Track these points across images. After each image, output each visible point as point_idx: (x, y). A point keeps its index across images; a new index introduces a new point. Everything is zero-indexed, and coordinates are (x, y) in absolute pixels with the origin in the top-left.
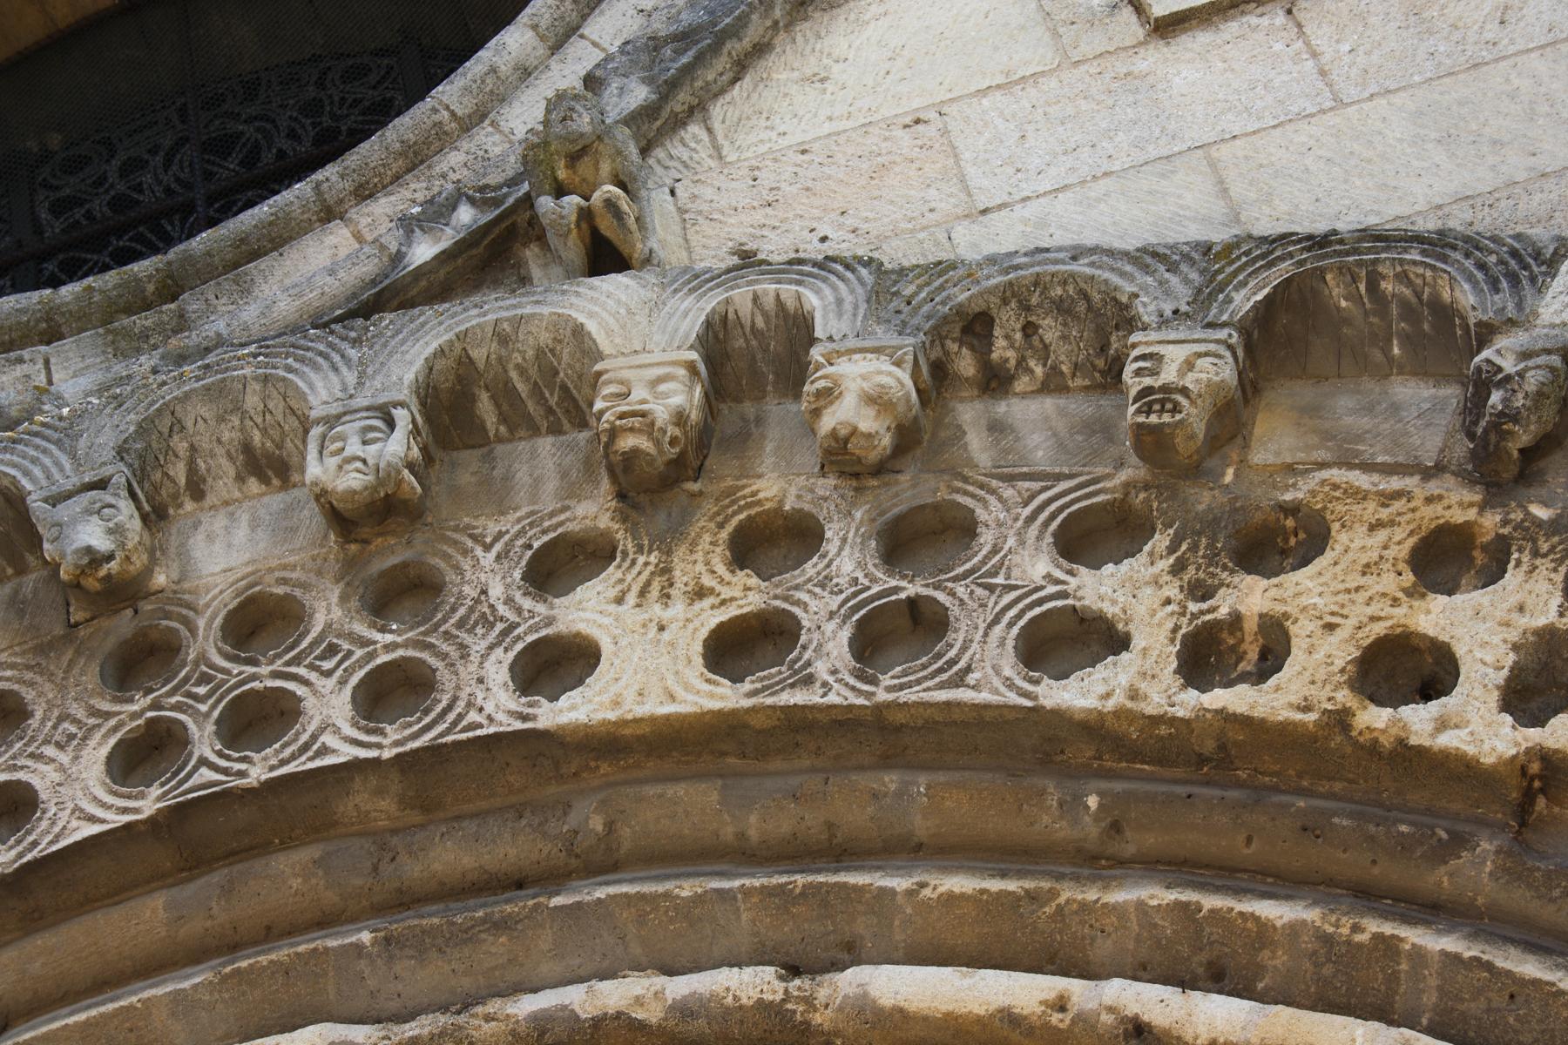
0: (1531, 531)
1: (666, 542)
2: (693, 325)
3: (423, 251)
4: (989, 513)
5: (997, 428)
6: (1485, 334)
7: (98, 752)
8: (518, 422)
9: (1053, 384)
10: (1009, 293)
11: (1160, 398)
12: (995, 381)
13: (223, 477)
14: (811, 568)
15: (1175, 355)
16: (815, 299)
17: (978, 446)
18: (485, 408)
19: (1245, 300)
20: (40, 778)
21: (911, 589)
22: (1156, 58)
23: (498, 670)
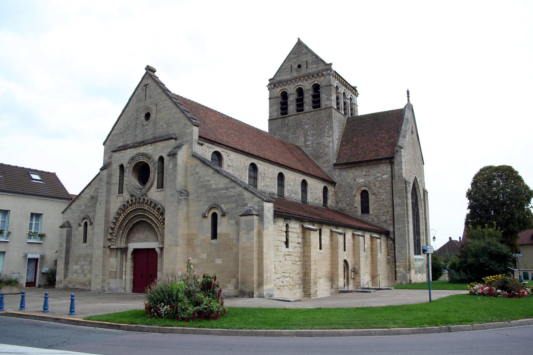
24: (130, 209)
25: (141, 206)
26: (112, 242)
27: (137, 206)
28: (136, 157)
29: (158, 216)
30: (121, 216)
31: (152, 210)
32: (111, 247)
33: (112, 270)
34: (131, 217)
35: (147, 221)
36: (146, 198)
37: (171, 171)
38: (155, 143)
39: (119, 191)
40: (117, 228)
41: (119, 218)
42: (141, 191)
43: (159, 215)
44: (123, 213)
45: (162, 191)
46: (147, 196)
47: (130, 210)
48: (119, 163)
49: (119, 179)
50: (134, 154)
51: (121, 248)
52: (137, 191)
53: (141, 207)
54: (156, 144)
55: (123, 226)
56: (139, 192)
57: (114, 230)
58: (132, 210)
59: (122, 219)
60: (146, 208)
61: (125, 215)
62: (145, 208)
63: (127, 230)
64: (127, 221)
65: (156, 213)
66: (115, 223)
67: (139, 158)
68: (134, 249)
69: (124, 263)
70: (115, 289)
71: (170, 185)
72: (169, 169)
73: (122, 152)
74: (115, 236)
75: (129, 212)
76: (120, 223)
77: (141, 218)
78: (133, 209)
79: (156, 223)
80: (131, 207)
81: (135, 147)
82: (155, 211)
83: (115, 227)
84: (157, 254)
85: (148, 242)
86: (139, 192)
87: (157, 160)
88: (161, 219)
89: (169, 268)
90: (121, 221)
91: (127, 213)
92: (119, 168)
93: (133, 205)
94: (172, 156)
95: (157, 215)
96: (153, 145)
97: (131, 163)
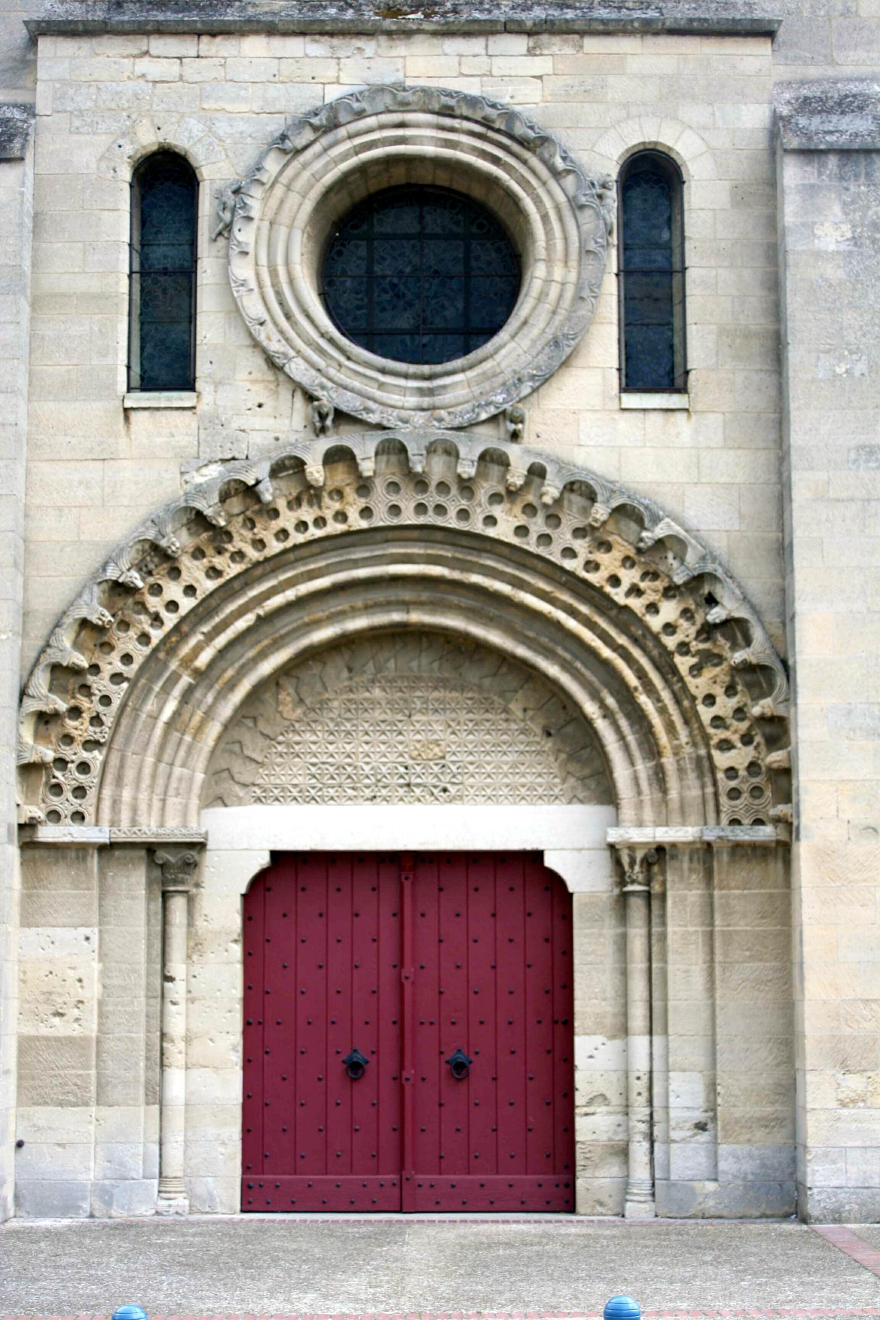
0: (640, 562)
1: (513, 502)
2: (527, 466)
3: (484, 416)
4: (564, 521)
5: (570, 501)
6: (644, 529)
7: (413, 505)
8: (492, 461)
9: (581, 495)
10: (580, 482)
11: (596, 520)
12: (572, 491)
13: (440, 451)
14: (534, 520)
15: (601, 511)
16: (549, 469)
17: (566, 503)
18: (488, 458)
19: (615, 504)
20: (402, 506)
21: (548, 531)
22: (619, 416)
23: (481, 518)
24: (302, 526)
25: (440, 509)
26: (57, 789)
27: (395, 510)
28: (360, 115)
29: (637, 604)
30: (175, 573)
31: (569, 553)
32: (48, 833)
33: (60, 1028)
34: (290, 594)
35: (478, 631)
36: (513, 451)
37: (834, 272)
38: (582, 33)
39: (129, 367)
40: (117, 678)
41: (157, 590)
42: (421, 392)
43: (650, 597)
44: (198, 553)
45: (681, 417)
46: (515, 436)
47: (297, 538)
48: (129, 133)
49: (127, 271)
50: (333, 94)
51: (150, 849)
52: (381, 386)
53: (430, 519)
54: (591, 44)
55: (186, 662)
56: (412, 401)
57: (86, 689)
58: (314, 532)
59: (187, 604)
60: (504, 531)
61: (233, 569)
62: (491, 532)
63: (221, 696)
64: (242, 624)
65: (615, 581)
66: (100, 630)
67: (402, 125)
68: (276, 855)
69: (177, 968)
70: (106, 1196)
71: (835, 375)
72: (818, 255)
73: (159, 45)
74: (91, 744)
75: (275, 547)
76: (157, 635)
77: (406, 605)
78: (334, 528)
79: (606, 652)
80: (307, 514)
81: (332, 34)
82: (609, 562)
83: (95, 669)
84: (567, 898)
85: (451, 800)
86: (412, 401)
87: (612, 170)
88: (670, 628)
89: (867, 1001)
90: (170, 620)
91: (253, 555)
92: (126, 174)
93: (339, 493)
94: (833, 161)
95: (635, 591)
96: (558, 46)
97: (306, 148)
